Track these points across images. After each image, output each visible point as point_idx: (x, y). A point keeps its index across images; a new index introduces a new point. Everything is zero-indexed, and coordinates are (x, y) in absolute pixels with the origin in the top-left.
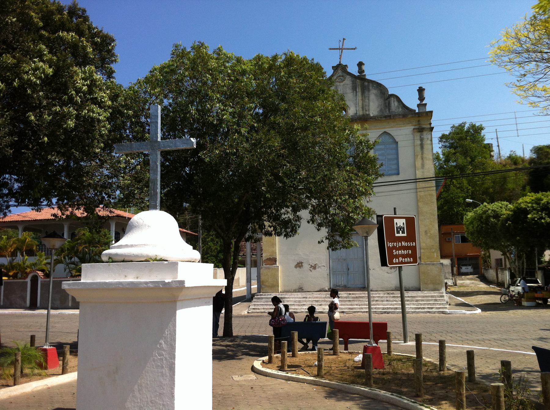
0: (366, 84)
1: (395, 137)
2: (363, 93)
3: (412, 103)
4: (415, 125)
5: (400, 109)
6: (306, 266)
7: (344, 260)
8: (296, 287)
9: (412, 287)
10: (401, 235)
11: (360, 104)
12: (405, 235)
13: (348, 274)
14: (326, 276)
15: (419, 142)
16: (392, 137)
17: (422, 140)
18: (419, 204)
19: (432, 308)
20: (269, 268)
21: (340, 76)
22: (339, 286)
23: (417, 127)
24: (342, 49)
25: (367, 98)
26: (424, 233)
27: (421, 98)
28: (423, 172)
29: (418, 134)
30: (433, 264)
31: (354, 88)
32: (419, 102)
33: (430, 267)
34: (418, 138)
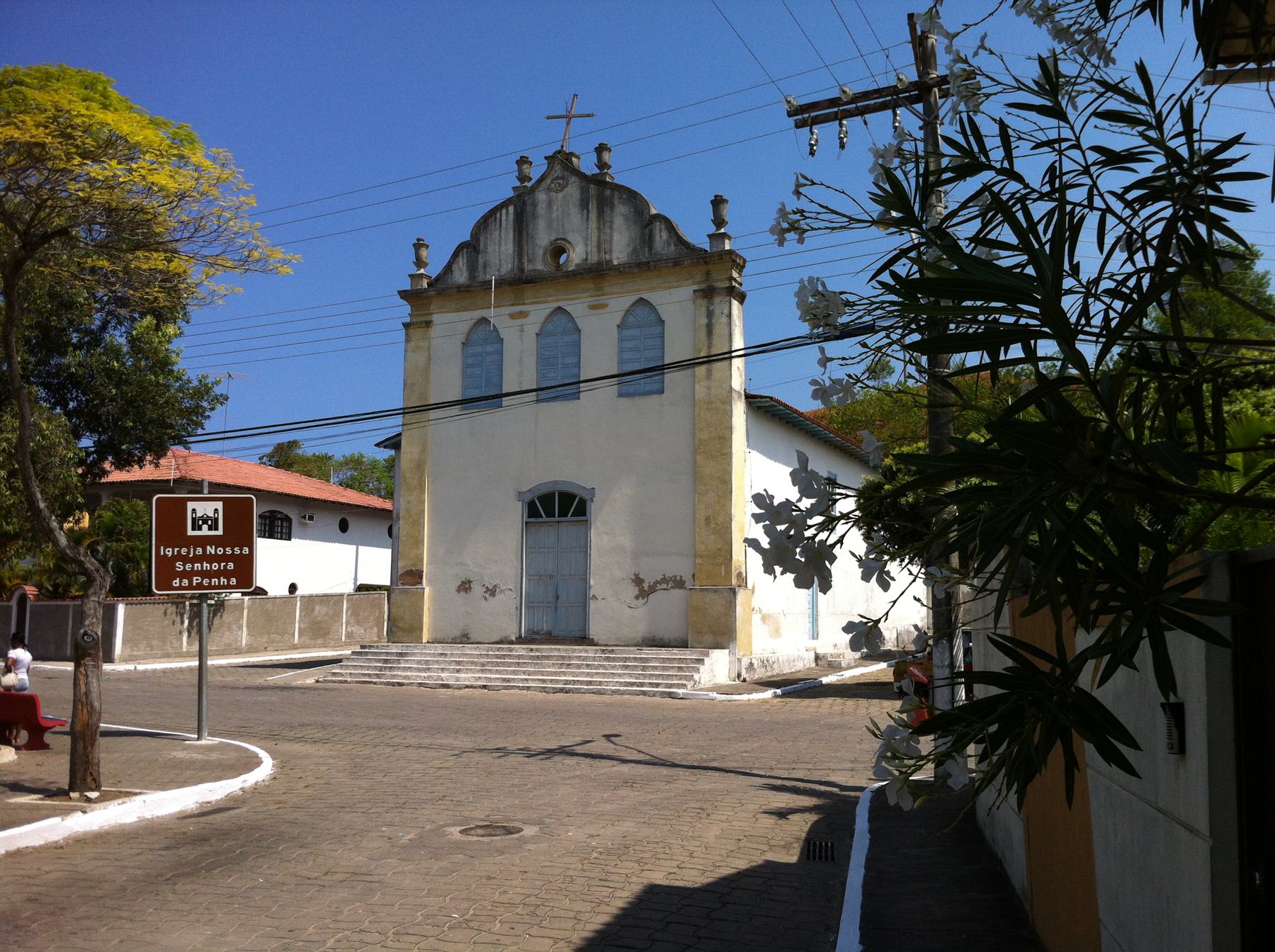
0: (608, 192)
1: (659, 309)
2: (601, 213)
3: (697, 232)
4: (699, 283)
5: (673, 247)
6: (477, 590)
7: (551, 577)
8: (456, 632)
9: (675, 640)
10: (205, 531)
11: (595, 239)
12: (220, 532)
13: (556, 608)
14: (513, 610)
15: (704, 321)
16: (571, 319)
17: (710, 315)
18: (698, 457)
19: (657, 685)
20: (406, 591)
21: (557, 178)
22: (537, 633)
23: (703, 286)
24: (568, 117)
25: (608, 225)
26: (703, 523)
27: (719, 221)
28: (709, 388)
29: (704, 303)
30: (716, 591)
31: (584, 204)
32: (712, 229)
33: (710, 597)
34: (704, 310)
